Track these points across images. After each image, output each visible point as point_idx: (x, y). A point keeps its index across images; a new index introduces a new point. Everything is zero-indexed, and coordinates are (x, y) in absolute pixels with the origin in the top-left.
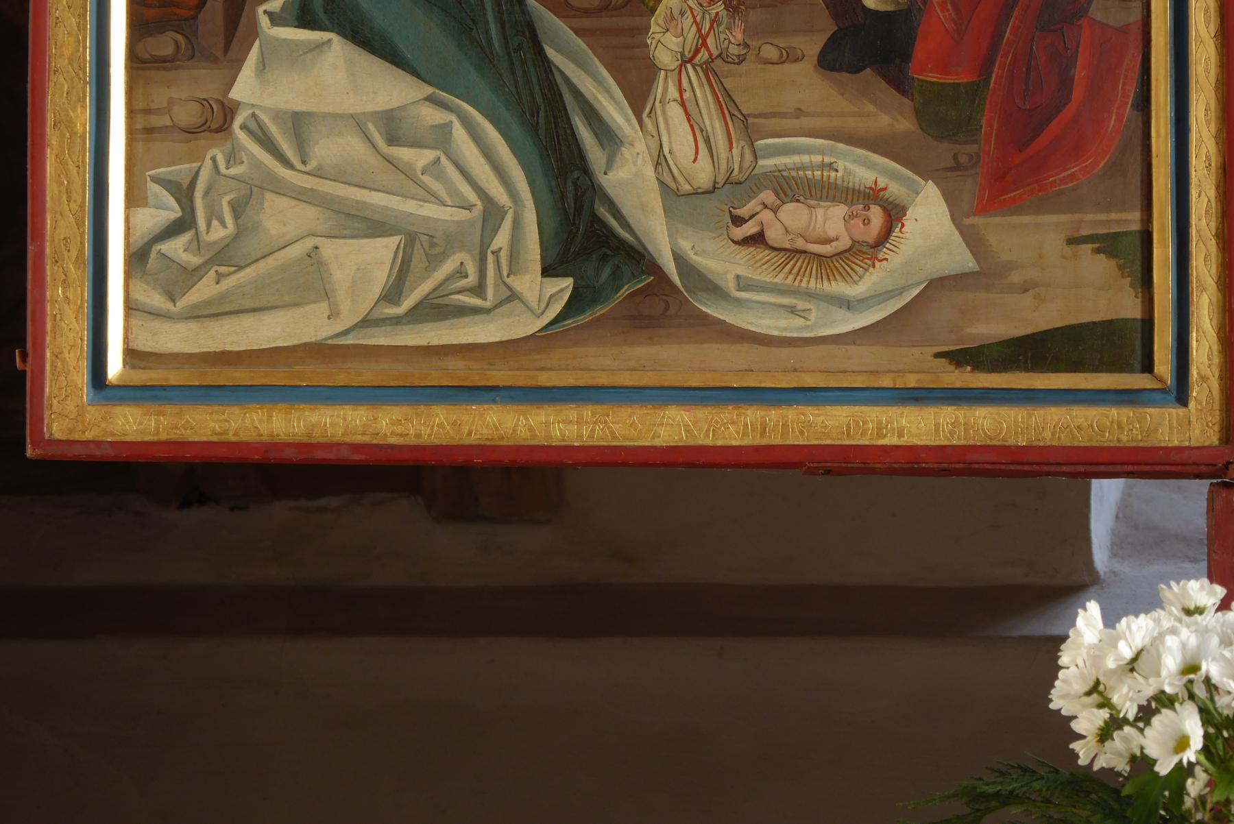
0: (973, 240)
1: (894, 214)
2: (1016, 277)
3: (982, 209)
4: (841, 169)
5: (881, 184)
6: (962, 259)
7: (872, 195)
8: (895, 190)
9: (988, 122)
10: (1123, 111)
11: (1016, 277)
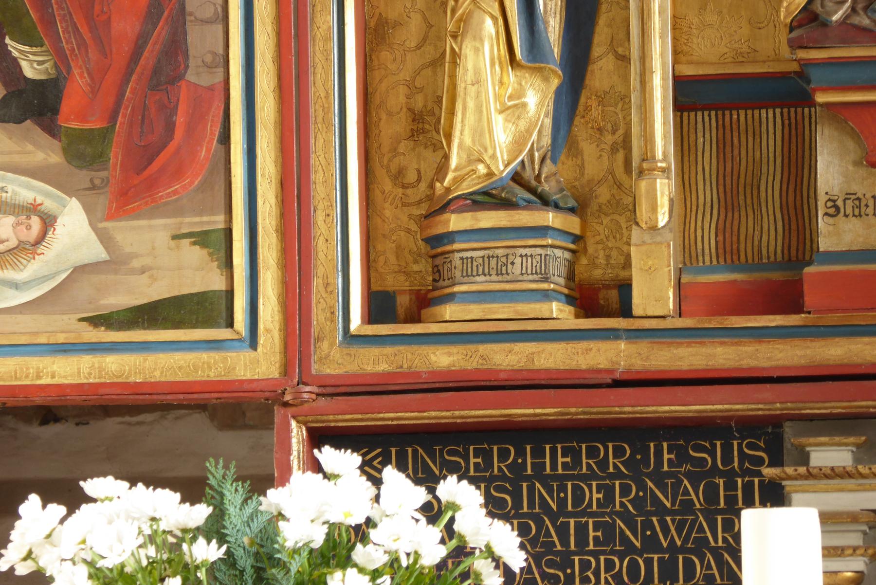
0: (105, 239)
1: (48, 222)
2: (136, 264)
3: (110, 217)
4: (10, 191)
5: (39, 201)
6: (98, 252)
7: (33, 209)
8: (49, 205)
9: (115, 155)
10: (210, 145)
11: (136, 264)
